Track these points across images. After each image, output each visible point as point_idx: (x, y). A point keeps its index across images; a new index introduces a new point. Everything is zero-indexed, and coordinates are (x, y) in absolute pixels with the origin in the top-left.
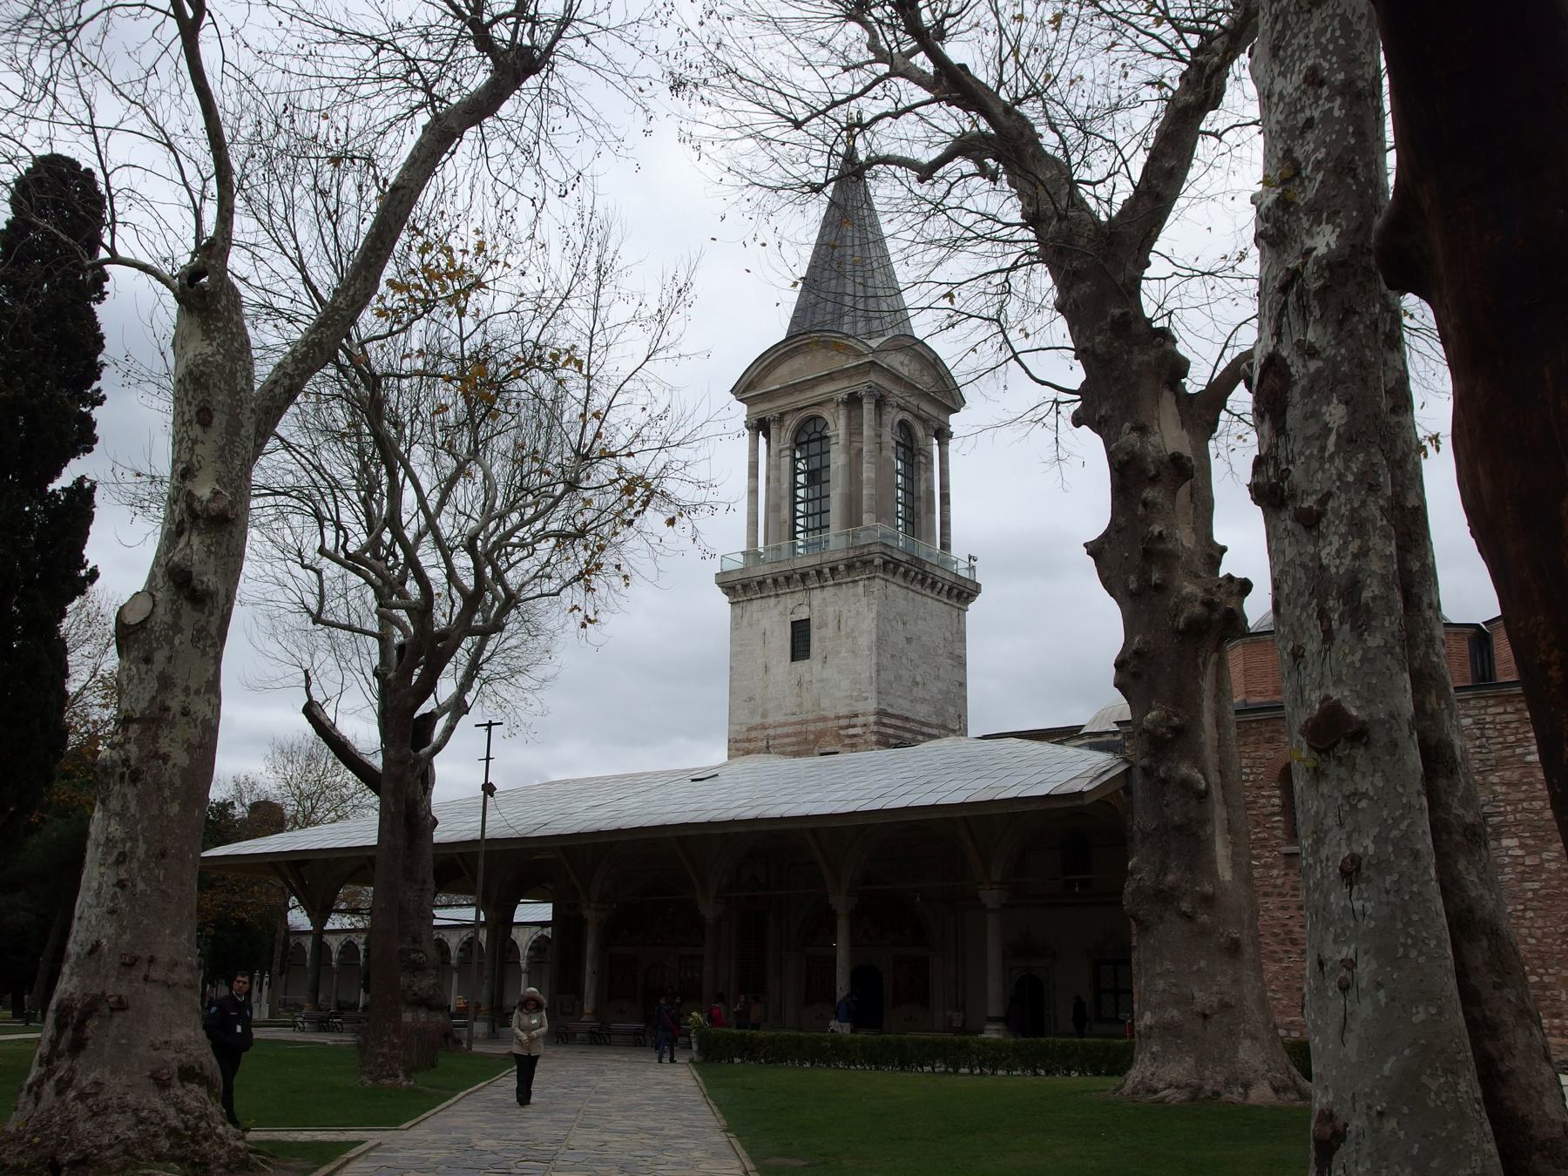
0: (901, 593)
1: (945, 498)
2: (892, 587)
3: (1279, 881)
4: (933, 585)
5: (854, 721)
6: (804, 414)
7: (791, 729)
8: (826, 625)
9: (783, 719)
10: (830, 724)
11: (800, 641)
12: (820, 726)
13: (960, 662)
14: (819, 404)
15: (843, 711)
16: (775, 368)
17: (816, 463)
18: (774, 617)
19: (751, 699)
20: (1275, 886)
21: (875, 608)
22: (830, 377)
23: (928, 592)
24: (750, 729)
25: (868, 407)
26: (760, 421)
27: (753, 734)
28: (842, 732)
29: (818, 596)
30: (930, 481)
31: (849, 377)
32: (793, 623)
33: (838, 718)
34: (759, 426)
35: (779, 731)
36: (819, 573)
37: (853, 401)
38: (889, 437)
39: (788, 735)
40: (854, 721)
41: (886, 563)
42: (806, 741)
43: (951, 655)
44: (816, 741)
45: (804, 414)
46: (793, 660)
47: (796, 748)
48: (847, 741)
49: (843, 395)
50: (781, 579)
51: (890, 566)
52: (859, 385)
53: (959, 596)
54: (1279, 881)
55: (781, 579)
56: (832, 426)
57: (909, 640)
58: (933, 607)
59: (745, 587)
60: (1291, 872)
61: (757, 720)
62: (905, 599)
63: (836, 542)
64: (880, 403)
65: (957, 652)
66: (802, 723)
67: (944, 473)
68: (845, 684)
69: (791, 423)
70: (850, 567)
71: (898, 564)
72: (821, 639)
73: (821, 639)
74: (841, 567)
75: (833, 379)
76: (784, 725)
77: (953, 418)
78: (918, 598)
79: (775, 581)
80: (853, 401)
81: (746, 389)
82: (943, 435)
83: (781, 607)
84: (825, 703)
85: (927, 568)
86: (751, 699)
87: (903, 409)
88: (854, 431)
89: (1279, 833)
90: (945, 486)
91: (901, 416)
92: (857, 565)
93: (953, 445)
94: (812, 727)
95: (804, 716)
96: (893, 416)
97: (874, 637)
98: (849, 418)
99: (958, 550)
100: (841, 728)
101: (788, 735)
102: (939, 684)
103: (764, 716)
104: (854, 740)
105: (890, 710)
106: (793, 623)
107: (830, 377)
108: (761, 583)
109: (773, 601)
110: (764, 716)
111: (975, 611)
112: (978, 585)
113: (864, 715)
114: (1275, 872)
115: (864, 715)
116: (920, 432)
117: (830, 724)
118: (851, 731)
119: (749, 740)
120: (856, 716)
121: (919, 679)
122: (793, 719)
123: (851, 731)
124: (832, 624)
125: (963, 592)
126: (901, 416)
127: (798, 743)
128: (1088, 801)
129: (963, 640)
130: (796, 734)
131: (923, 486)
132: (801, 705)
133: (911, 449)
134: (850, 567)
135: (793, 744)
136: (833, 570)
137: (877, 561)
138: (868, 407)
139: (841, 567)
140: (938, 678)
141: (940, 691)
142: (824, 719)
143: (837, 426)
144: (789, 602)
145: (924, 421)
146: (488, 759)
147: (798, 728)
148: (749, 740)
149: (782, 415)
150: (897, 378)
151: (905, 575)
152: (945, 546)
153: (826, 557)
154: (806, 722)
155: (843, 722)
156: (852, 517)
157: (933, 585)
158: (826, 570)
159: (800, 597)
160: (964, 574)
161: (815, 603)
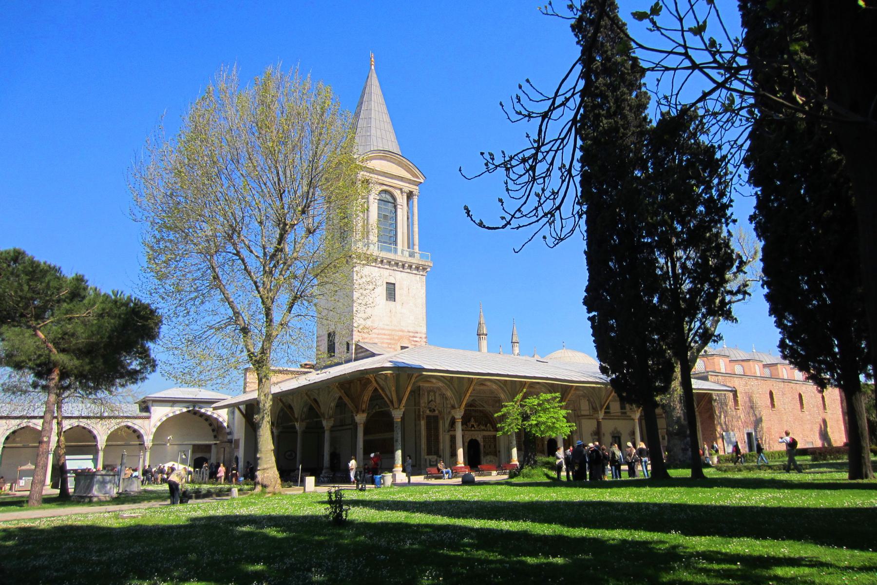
6: (385, 187)
7: (387, 332)
11: (391, 291)
12: (401, 333)
15: (411, 329)
22: (401, 179)
35: (381, 331)
36: (403, 266)
42: (394, 339)
44: (399, 340)
49: (406, 190)
55: (385, 261)
66: (393, 330)
76: (383, 329)
79: (382, 262)
80: (410, 195)
94: (398, 333)
107: (401, 179)
122: (386, 327)
142: (403, 331)
143: (401, 200)
144: (386, 273)
147: (390, 332)
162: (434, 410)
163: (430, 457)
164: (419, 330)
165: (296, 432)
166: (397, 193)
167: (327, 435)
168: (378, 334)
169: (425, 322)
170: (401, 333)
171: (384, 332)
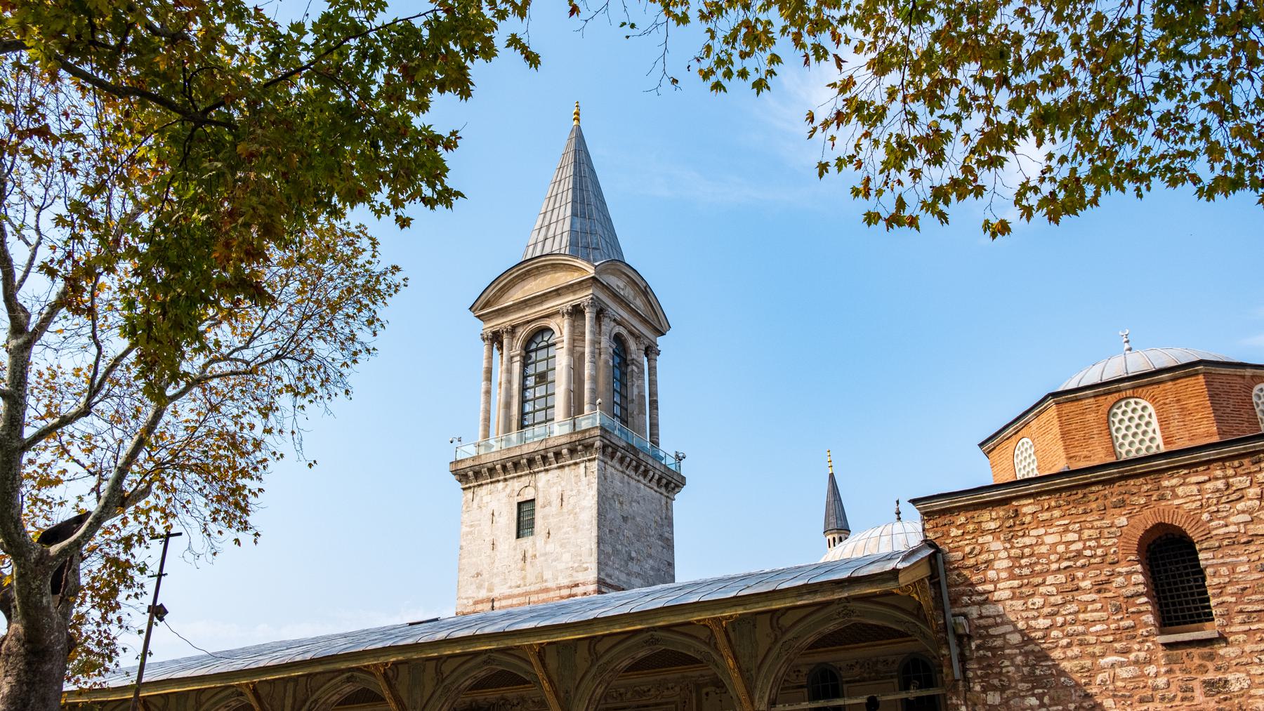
0: (618, 475)
1: (654, 404)
2: (610, 469)
3: (1161, 681)
4: (645, 473)
6: (533, 325)
8: (550, 503)
10: (552, 594)
13: (669, 544)
14: (548, 316)
15: (565, 581)
16: (509, 289)
17: (541, 367)
18: (499, 499)
19: (478, 574)
20: (1155, 688)
21: (595, 486)
23: (641, 478)
24: (476, 603)
25: (589, 315)
26: (494, 333)
29: (543, 478)
30: (641, 387)
31: (574, 292)
32: (519, 504)
33: (560, 588)
34: (495, 339)
36: (544, 458)
37: (576, 312)
38: (605, 342)
40: (575, 590)
41: (604, 447)
43: (661, 537)
45: (533, 325)
46: (518, 537)
50: (509, 464)
51: (609, 450)
52: (584, 297)
53: (667, 486)
54: (1161, 681)
55: (509, 464)
56: (557, 334)
57: (625, 519)
58: (646, 490)
59: (477, 475)
60: (1176, 667)
61: (483, 594)
62: (622, 482)
63: (560, 430)
64: (600, 314)
65: (666, 535)
67: (653, 383)
68: (566, 557)
69: (522, 333)
70: (572, 451)
71: (616, 449)
73: (544, 517)
74: (565, 451)
75: (559, 295)
76: (510, 597)
77: (660, 340)
78: (633, 483)
79: (504, 468)
80: (576, 312)
81: (485, 306)
82: (651, 351)
83: (508, 490)
84: (548, 575)
85: (641, 456)
86: (478, 574)
87: (619, 324)
88: (576, 338)
89: (1149, 618)
90: (653, 393)
91: (618, 329)
92: (578, 448)
93: (660, 362)
95: (528, 588)
96: (607, 326)
97: (594, 512)
98: (573, 327)
99: (667, 446)
102: (651, 562)
103: (490, 590)
105: (608, 581)
106: (519, 504)
107: (558, 292)
108: (492, 471)
109: (501, 485)
110: (490, 590)
111: (681, 502)
112: (684, 478)
113: (584, 584)
114: (1152, 669)
115: (584, 584)
116: (632, 344)
120: (577, 585)
121: (633, 554)
122: (516, 591)
124: (556, 502)
125: (671, 483)
126: (618, 329)
128: (903, 580)
129: (671, 525)
131: (636, 391)
132: (524, 578)
133: (625, 360)
134: (572, 451)
136: (558, 455)
137: (598, 444)
138: (589, 315)
139: (565, 451)
140: (650, 556)
141: (652, 568)
142: (547, 590)
144: (516, 485)
145: (637, 337)
146: (160, 575)
147: (522, 599)
149: (514, 328)
150: (616, 296)
151: (622, 460)
152: (655, 443)
153: (551, 443)
155: (565, 592)
156: (575, 407)
157: (645, 473)
158: (551, 455)
159: (525, 480)
160: (670, 462)
161: (540, 485)
164: (580, 577)
166: (552, 323)
169: (595, 556)
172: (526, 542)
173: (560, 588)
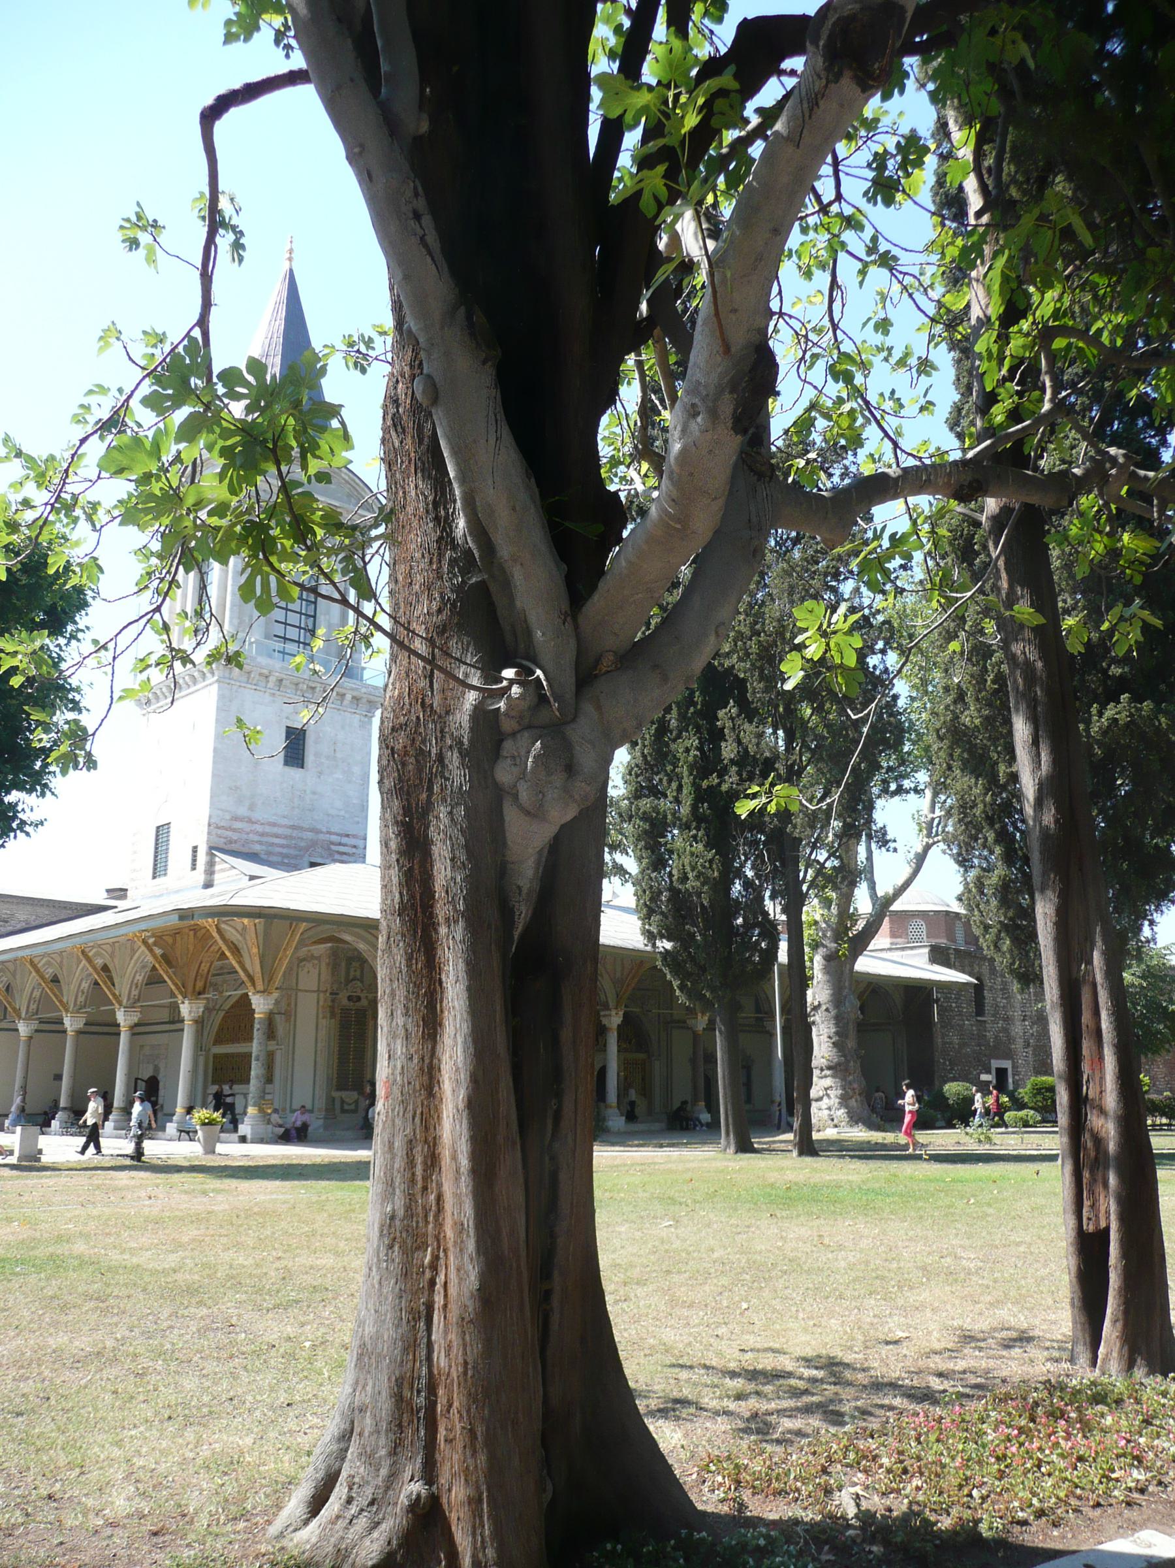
5: (345, 840)
7: (280, 831)
9: (273, 819)
10: (321, 837)
11: (295, 747)
12: (310, 835)
24: (236, 818)
27: (238, 825)
28: (333, 847)
33: (329, 833)
35: (268, 829)
39: (277, 836)
40: (345, 840)
47: (285, 851)
48: (337, 857)
61: (242, 811)
66: (293, 827)
72: (317, 755)
73: (317, 755)
74: (349, 697)
76: (274, 825)
100: (332, 843)
101: (277, 836)
103: (252, 808)
104: (345, 858)
109: (267, 698)
117: (321, 837)
118: (342, 849)
119: (234, 830)
120: (348, 836)
123: (342, 849)
127: (288, 846)
130: (286, 837)
135: (282, 846)
139: (349, 697)
142: (317, 831)
147: (288, 832)
148: (234, 830)
154: (301, 828)
155: (334, 838)
162: (359, 999)
163: (344, 1094)
165: (65, 1032)
167: (124, 1039)
168: (262, 835)
170: (310, 835)
171: (275, 830)
172: (294, 773)
173: (329, 833)
